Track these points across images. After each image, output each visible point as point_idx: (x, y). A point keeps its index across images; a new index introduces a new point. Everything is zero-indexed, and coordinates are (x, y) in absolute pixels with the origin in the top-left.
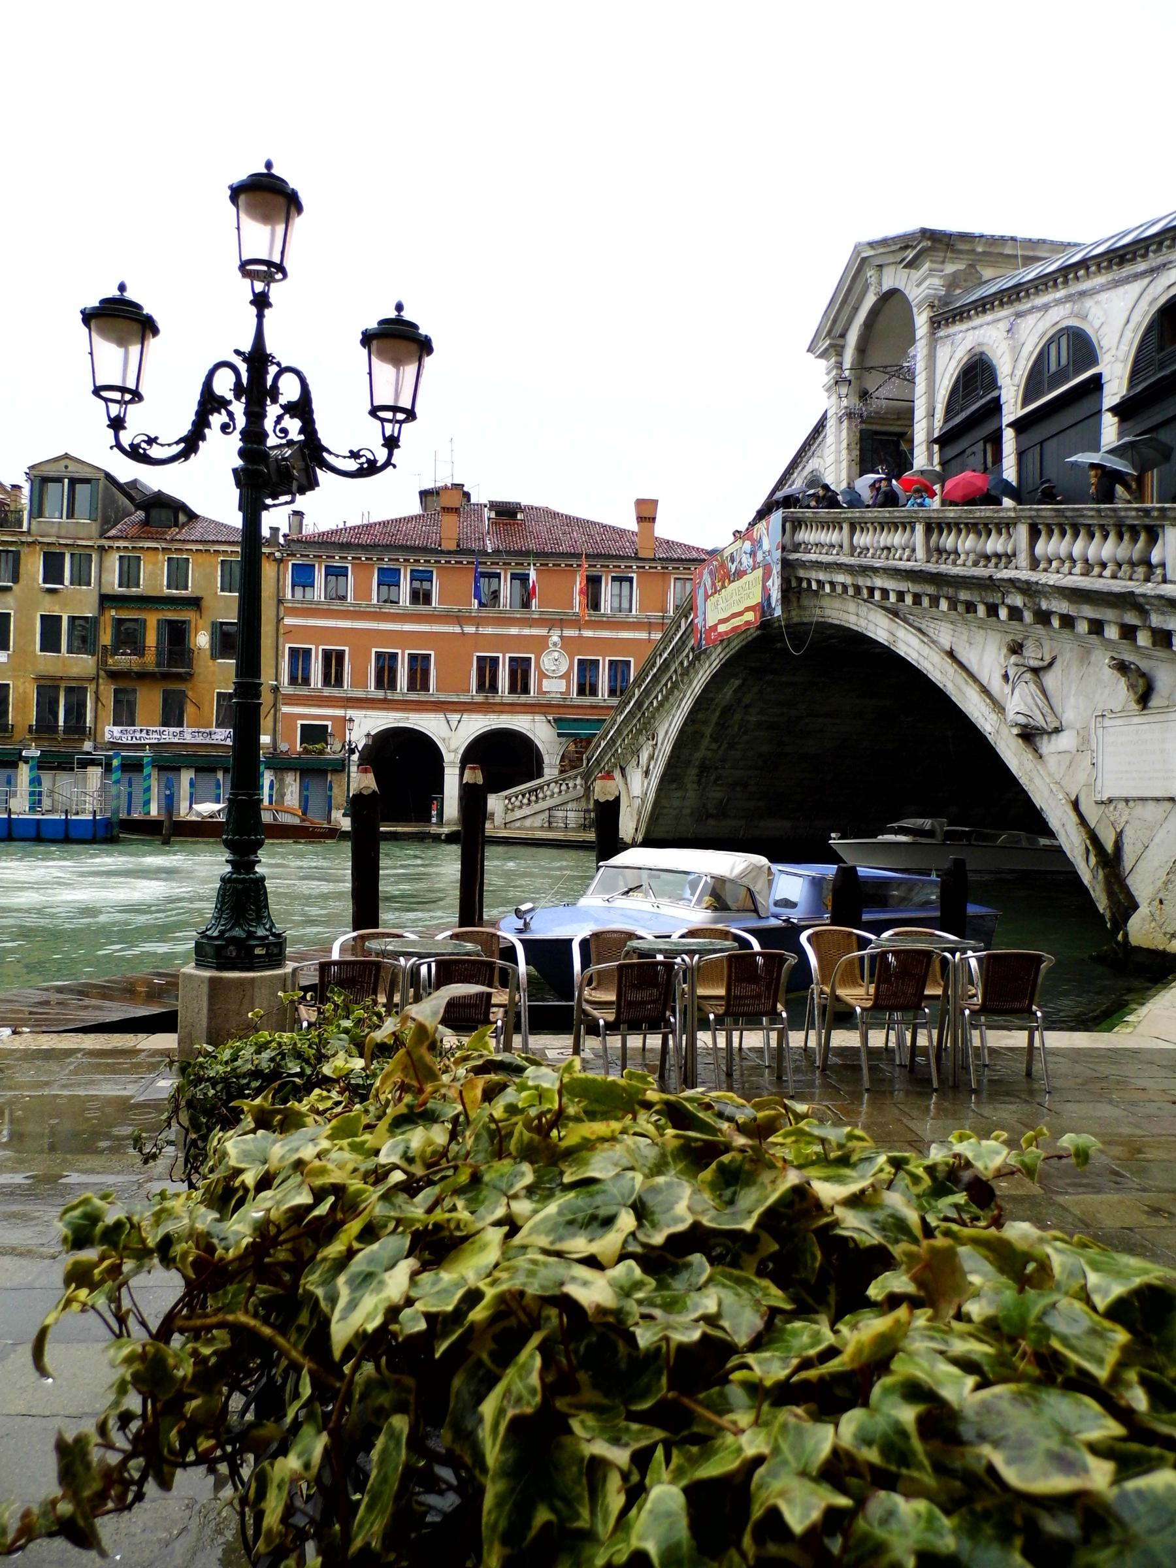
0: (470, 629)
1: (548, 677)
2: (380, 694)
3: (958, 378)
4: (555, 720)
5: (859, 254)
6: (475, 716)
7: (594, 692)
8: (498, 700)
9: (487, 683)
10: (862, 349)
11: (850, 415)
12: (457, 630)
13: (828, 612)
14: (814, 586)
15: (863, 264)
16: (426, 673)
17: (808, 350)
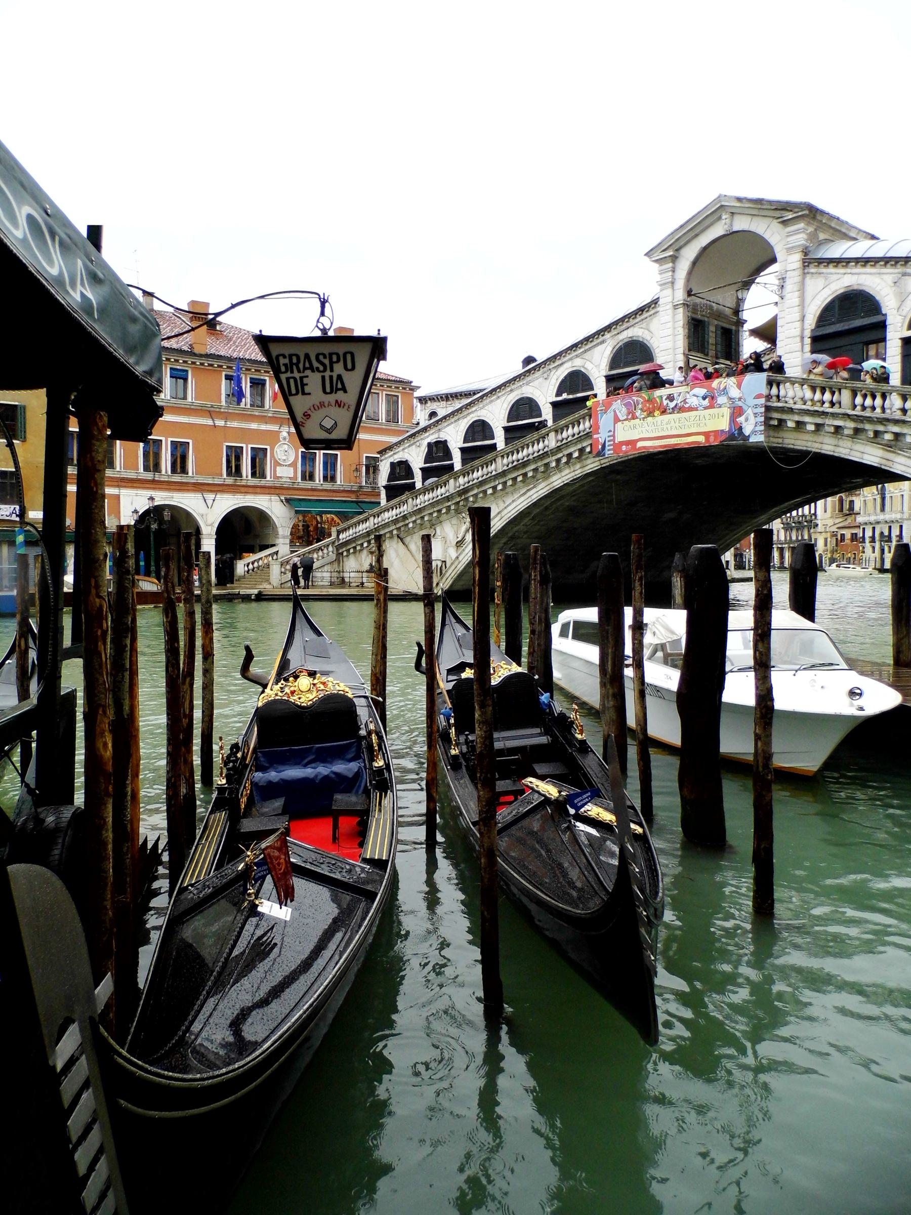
0: (220, 423)
1: (281, 465)
2: (149, 476)
3: (832, 302)
4: (288, 500)
5: (720, 201)
6: (226, 496)
7: (312, 477)
8: (244, 483)
9: (235, 470)
10: (694, 263)
11: (685, 305)
12: (210, 422)
13: (786, 441)
14: (791, 424)
15: (718, 210)
16: (184, 458)
17: (646, 255)
